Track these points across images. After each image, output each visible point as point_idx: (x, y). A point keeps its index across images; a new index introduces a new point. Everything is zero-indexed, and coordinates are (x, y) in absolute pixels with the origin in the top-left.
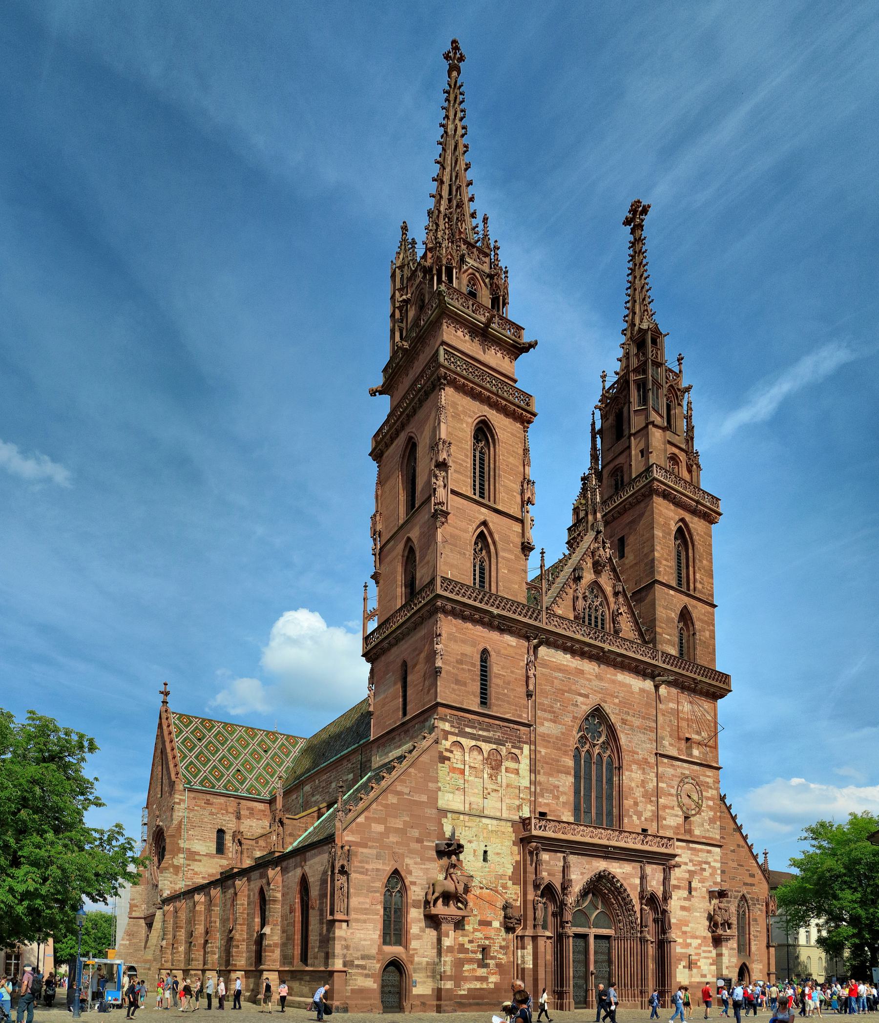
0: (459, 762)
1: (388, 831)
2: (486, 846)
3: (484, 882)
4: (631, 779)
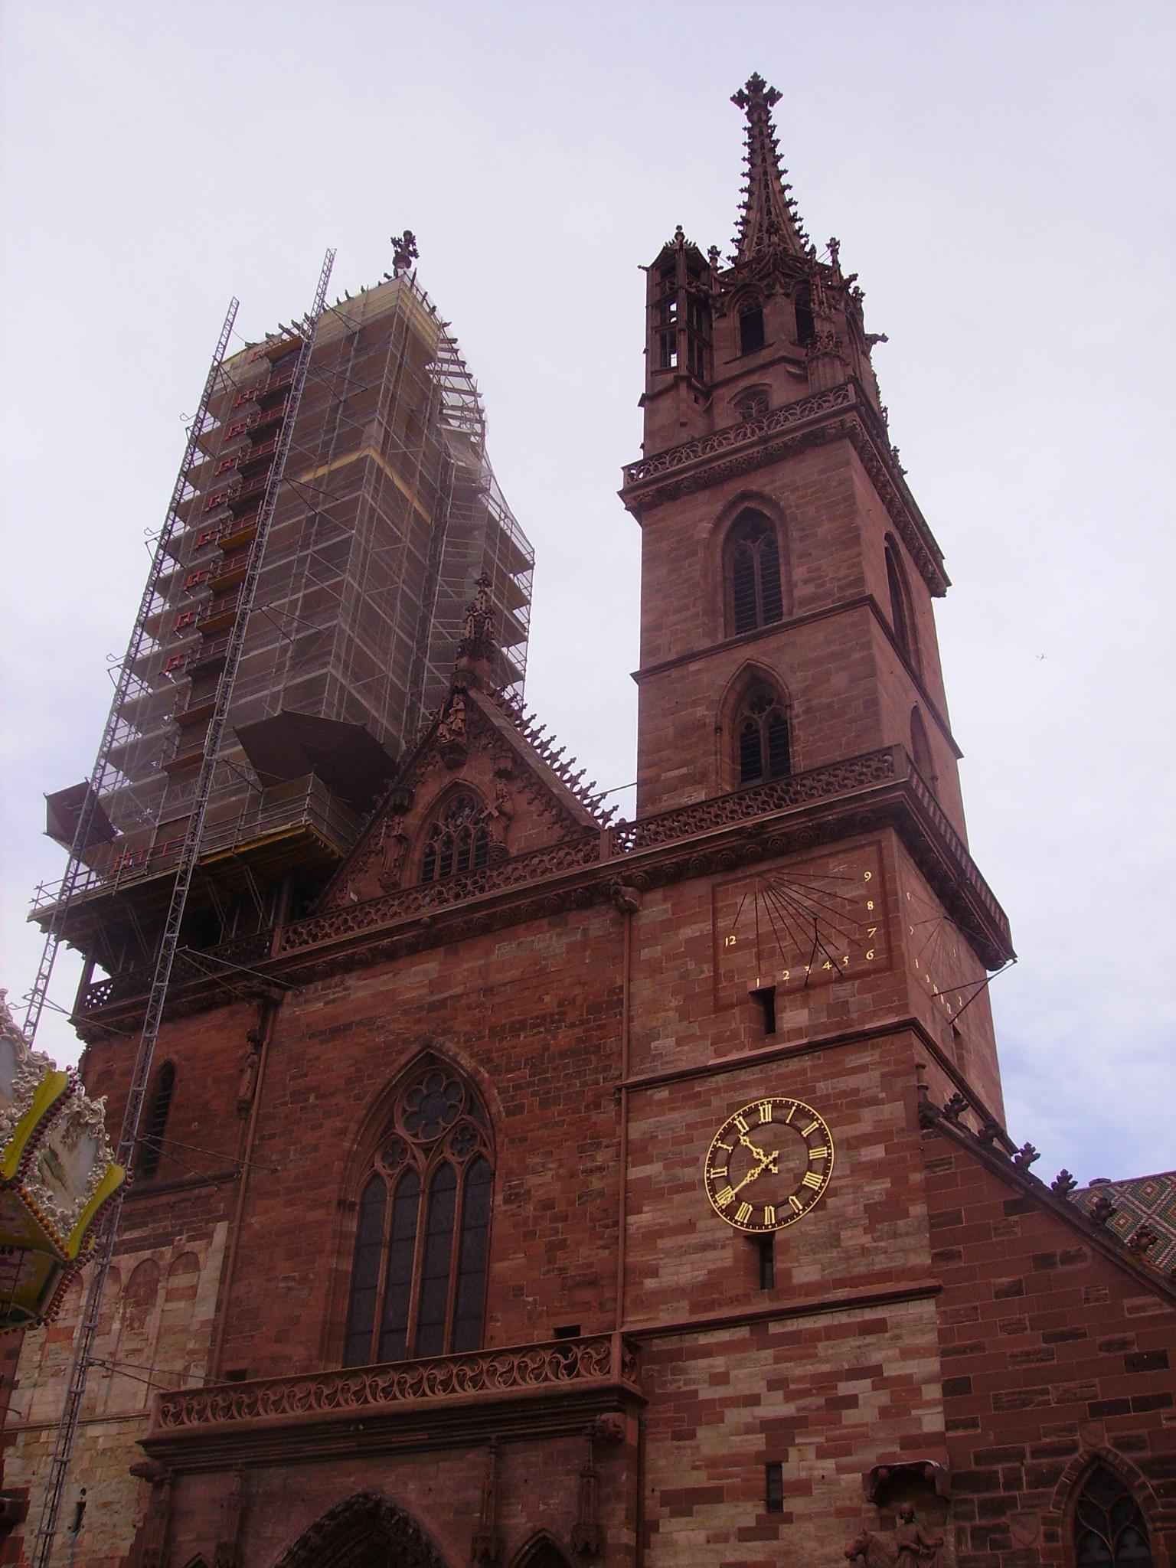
0: (71, 1314)
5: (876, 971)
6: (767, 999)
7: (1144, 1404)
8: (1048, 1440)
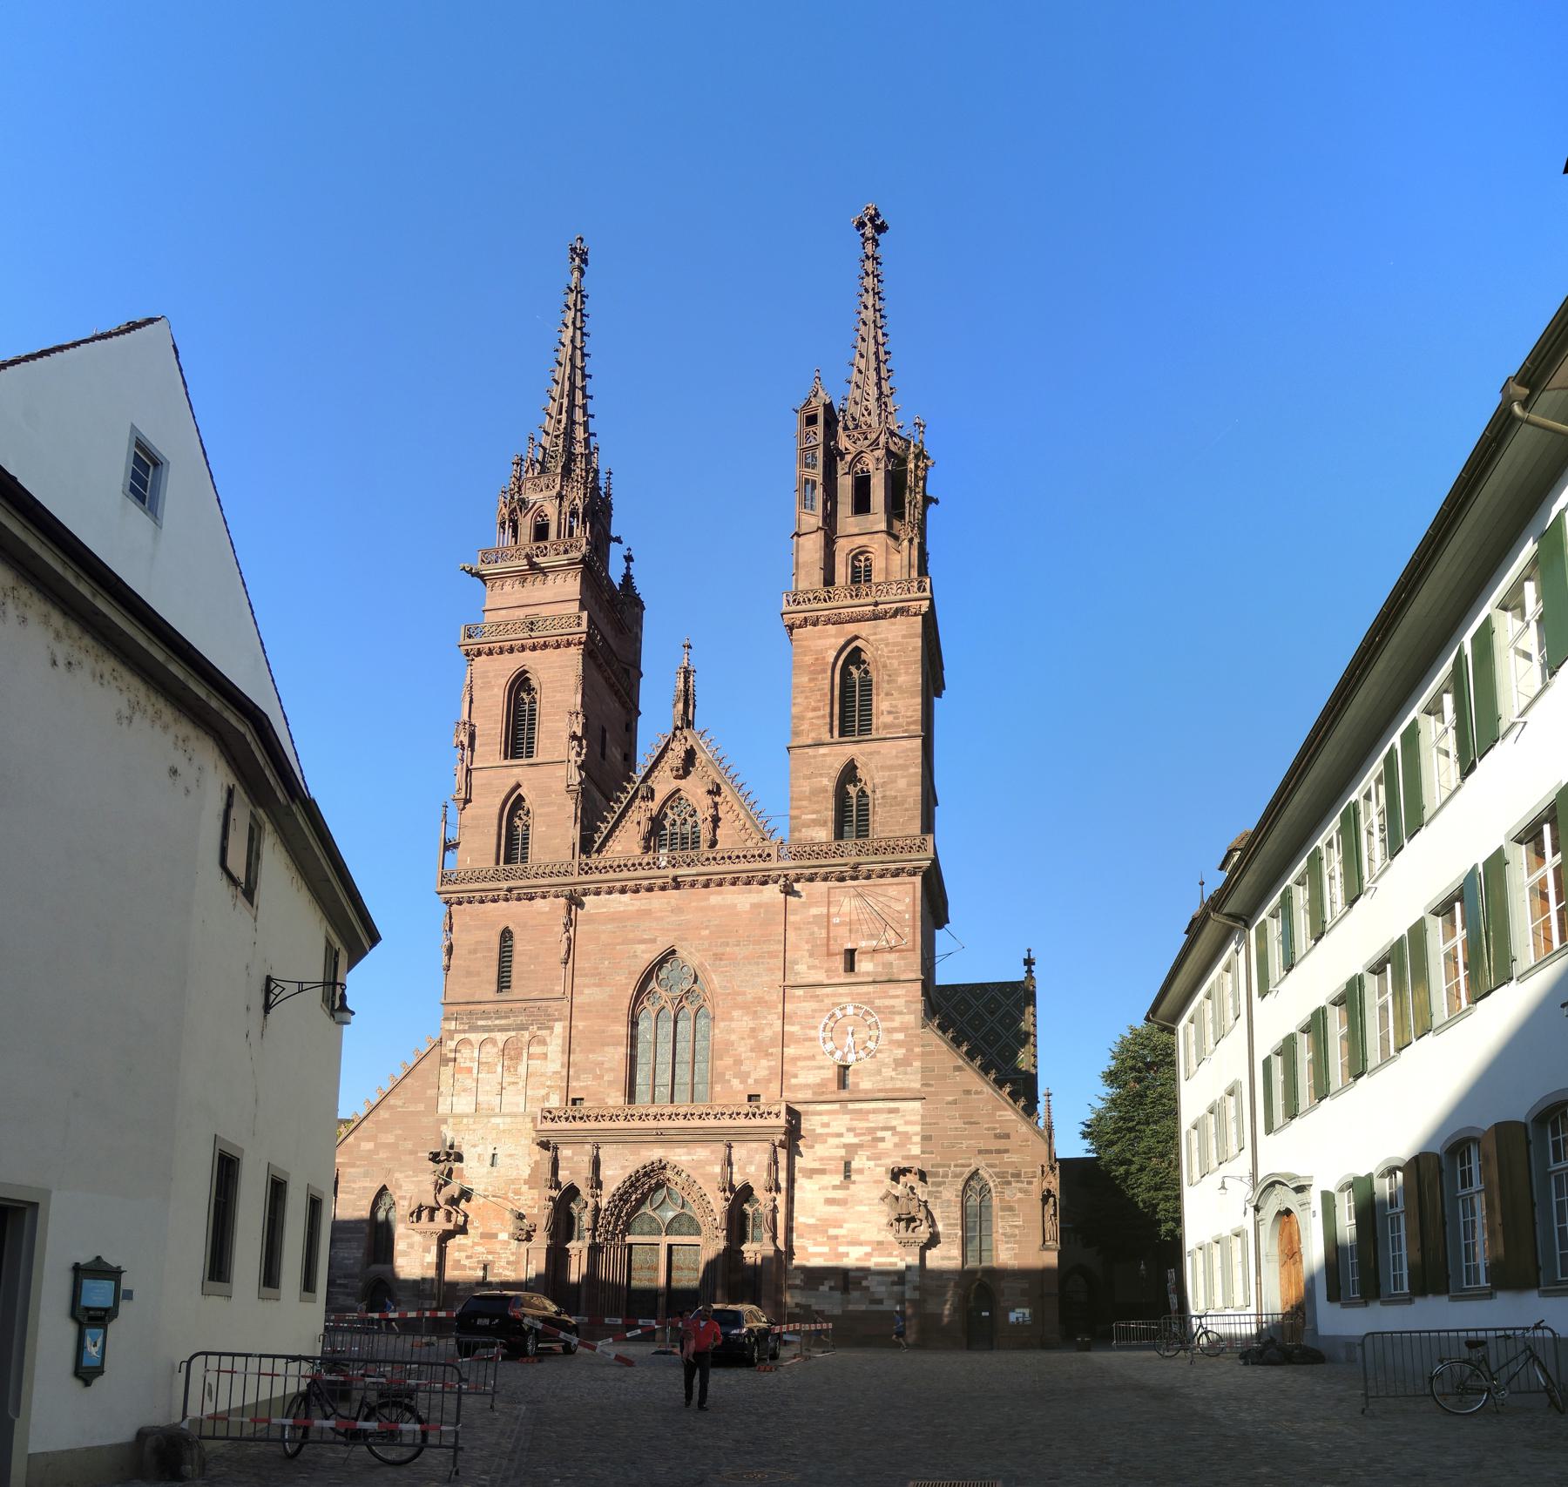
0: (468, 1061)
1: (378, 1146)
2: (495, 1148)
3: (490, 1189)
4: (731, 1031)
5: (907, 950)
6: (850, 954)
7: (999, 1152)
8: (960, 1161)
